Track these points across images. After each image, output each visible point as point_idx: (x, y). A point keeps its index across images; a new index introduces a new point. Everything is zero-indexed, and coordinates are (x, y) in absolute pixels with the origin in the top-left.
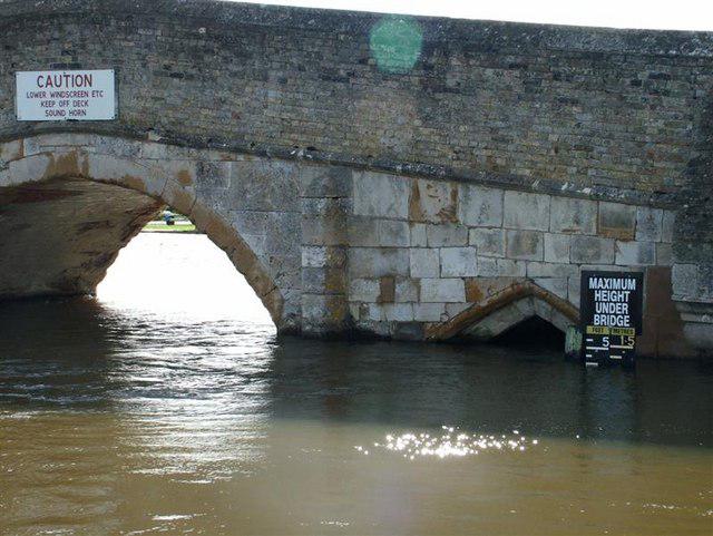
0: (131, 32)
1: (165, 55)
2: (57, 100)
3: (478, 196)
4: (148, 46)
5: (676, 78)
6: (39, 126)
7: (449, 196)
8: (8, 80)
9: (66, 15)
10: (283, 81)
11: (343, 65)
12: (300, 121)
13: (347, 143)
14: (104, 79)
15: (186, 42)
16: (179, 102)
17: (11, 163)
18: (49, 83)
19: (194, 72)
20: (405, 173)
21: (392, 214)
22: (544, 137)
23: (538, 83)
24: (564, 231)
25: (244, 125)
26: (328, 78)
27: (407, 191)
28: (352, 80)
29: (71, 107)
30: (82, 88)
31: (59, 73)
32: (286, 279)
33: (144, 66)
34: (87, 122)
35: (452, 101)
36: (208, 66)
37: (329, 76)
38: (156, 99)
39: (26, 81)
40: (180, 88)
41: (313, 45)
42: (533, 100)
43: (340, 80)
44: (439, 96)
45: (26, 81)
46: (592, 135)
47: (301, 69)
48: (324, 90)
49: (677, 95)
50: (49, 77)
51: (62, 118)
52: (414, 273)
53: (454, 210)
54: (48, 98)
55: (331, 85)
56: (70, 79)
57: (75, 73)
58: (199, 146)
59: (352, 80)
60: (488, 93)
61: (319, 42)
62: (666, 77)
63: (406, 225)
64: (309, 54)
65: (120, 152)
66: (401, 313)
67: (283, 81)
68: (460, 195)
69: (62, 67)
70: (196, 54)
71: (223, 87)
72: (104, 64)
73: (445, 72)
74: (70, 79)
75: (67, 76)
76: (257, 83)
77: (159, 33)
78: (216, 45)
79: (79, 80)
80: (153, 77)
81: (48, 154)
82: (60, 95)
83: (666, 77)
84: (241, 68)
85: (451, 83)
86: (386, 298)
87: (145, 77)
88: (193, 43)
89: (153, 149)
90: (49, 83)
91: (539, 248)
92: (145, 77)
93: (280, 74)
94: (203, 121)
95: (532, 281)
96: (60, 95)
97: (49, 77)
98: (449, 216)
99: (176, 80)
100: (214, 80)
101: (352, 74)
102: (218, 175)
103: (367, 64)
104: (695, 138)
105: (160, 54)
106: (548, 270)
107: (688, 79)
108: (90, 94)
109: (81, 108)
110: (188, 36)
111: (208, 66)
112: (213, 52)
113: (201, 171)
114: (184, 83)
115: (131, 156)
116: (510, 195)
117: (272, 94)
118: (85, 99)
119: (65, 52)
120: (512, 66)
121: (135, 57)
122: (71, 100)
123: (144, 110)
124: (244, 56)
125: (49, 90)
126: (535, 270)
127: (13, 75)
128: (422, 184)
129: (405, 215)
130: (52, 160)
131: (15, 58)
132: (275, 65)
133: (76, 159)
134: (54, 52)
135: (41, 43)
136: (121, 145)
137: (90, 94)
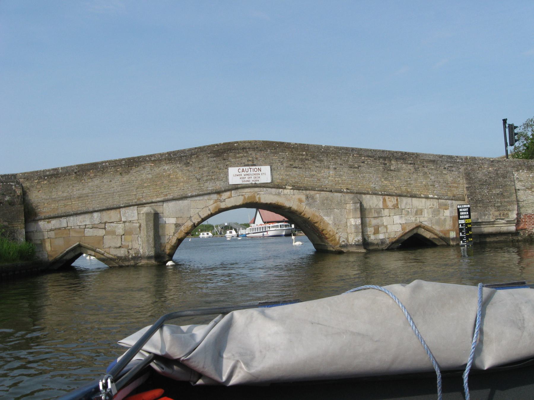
0: (276, 154)
1: (290, 161)
2: (247, 177)
3: (405, 200)
4: (283, 158)
5: (454, 167)
6: (239, 186)
7: (395, 200)
8: (225, 170)
9: (249, 148)
10: (335, 169)
11: (357, 164)
12: (342, 180)
13: (360, 187)
14: (266, 169)
15: (298, 157)
17: (226, 200)
18: (243, 171)
19: (300, 166)
20: (382, 195)
21: (377, 207)
22: (422, 183)
23: (418, 168)
24: (430, 208)
25: (321, 182)
26: (351, 167)
27: (382, 200)
28: (360, 168)
29: (253, 179)
30: (257, 172)
31: (247, 168)
32: (340, 230)
34: (260, 184)
35: (393, 174)
36: (307, 164)
37: (351, 167)
38: (287, 175)
41: (345, 158)
42: (417, 173)
43: (356, 168)
44: (389, 172)
46: (435, 182)
47: (341, 164)
48: (351, 171)
49: (455, 171)
50: (243, 169)
51: (249, 183)
52: (385, 224)
53: (397, 204)
54: (243, 176)
55: (353, 169)
56: (252, 170)
57: (254, 167)
58: (306, 189)
59: (360, 168)
60: (404, 171)
62: (452, 167)
63: (382, 210)
64: (344, 160)
65: (274, 193)
66: (381, 236)
67: (335, 169)
68: (399, 200)
69: (248, 165)
70: (302, 160)
71: (313, 171)
72: (265, 164)
73: (390, 165)
74: (252, 170)
75: (251, 169)
76: (325, 169)
77: (287, 154)
78: (310, 158)
79: (256, 170)
80: (285, 168)
81: (242, 195)
82: (247, 175)
83: (452, 167)
84: (319, 165)
85: (392, 168)
87: (282, 168)
88: (301, 157)
89: (288, 191)
90: (243, 171)
91: (423, 213)
92: (282, 168)
93: (334, 166)
94: (307, 181)
95: (421, 223)
96: (247, 175)
97: (243, 169)
98: (396, 206)
99: (295, 169)
100: (310, 168)
101: (360, 166)
102: (313, 198)
103: (364, 163)
104: (465, 182)
106: (426, 219)
107: (457, 167)
108: (261, 174)
109: (257, 179)
110: (299, 155)
111: (307, 164)
113: (307, 197)
114: (297, 170)
115: (279, 194)
116: (414, 199)
117: (331, 172)
118: (259, 176)
120: (411, 164)
121: (278, 162)
122: (253, 177)
123: (282, 179)
124: (321, 161)
125: (243, 173)
126: (422, 219)
127: (227, 168)
128: (387, 197)
129: (382, 207)
130: (245, 198)
131: (228, 163)
132: (332, 164)
133: (255, 197)
134: (244, 160)
135: (239, 158)
136: (274, 190)
137: (261, 174)
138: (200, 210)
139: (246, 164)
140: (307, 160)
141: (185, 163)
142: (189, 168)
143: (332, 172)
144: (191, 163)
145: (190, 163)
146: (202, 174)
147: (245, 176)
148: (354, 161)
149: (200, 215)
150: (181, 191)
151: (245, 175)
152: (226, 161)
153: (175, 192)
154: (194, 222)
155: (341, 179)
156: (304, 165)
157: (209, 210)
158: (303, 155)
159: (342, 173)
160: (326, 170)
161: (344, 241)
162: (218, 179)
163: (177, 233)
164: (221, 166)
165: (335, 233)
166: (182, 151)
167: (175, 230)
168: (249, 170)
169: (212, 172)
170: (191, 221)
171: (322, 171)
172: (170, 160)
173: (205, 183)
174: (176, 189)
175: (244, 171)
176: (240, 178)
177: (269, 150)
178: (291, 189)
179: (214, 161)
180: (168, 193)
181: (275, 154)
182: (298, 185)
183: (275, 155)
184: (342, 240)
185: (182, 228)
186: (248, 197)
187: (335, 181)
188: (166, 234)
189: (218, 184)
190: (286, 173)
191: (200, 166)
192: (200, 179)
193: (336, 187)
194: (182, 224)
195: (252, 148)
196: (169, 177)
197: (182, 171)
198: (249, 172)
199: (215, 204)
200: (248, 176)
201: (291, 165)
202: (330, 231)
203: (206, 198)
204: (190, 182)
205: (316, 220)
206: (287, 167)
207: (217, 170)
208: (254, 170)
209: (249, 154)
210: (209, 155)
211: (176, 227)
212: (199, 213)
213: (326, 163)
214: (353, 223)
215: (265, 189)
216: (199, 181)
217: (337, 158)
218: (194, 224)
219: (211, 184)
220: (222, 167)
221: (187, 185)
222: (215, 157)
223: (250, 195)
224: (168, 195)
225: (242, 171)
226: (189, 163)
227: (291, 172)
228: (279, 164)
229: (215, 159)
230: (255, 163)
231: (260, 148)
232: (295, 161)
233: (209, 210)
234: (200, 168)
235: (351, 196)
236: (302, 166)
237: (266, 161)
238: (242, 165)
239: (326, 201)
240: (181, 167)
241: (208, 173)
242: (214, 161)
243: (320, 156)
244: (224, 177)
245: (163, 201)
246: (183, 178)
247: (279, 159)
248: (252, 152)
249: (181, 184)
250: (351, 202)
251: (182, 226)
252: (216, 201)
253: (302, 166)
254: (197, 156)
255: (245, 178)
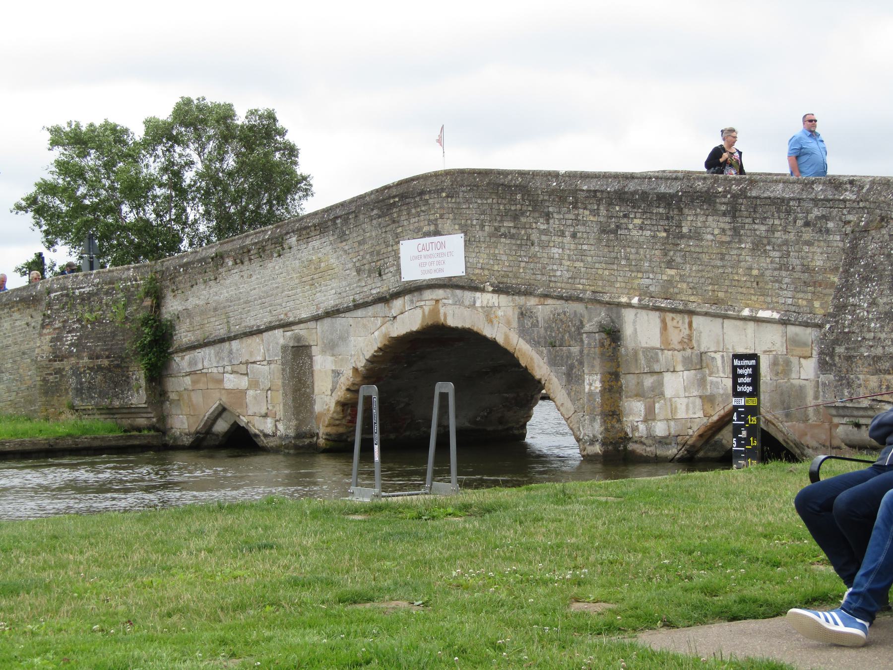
7: (687, 326)
14: (455, 242)
30: (441, 251)
39: (408, 249)
45: (408, 249)
53: (690, 338)
58: (519, 293)
63: (660, 352)
66: (660, 429)
70: (515, 217)
86: (650, 416)
109: (441, 267)
124: (548, 216)
128: (669, 316)
129: (658, 346)
202: (562, 404)
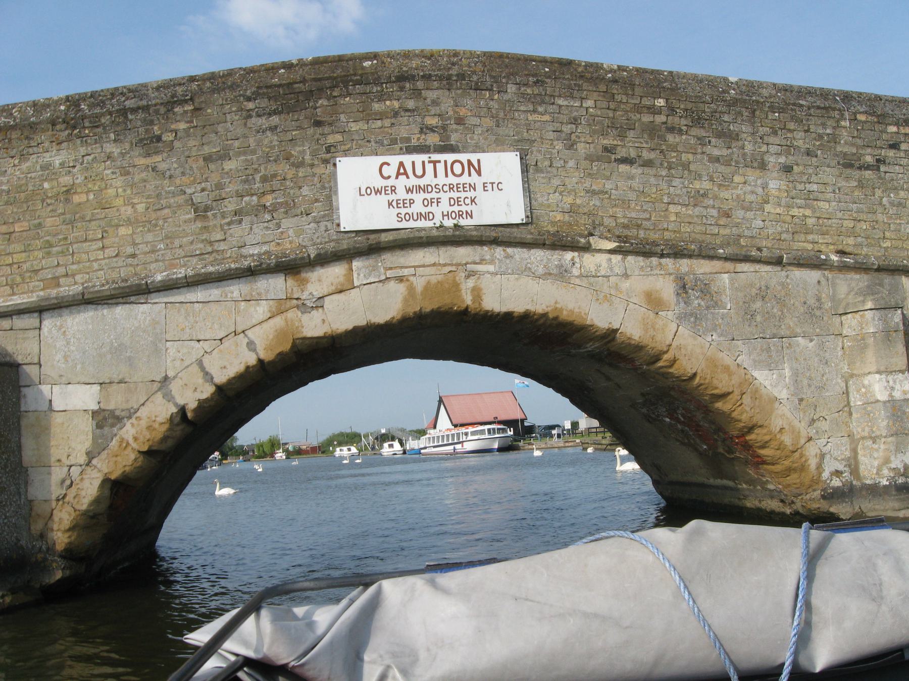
0: (543, 102)
1: (604, 134)
2: (419, 197)
4: (575, 121)
6: (384, 238)
8: (320, 170)
9: (427, 77)
10: (788, 169)
11: (869, 150)
13: (887, 244)
15: (635, 117)
16: (632, 196)
17: (326, 299)
18: (401, 171)
19: (646, 155)
25: (737, 225)
26: (849, 166)
28: (883, 168)
29: (445, 207)
30: (465, 179)
31: (418, 158)
32: (823, 425)
33: (571, 146)
36: (674, 148)
37: (849, 163)
38: (594, 193)
40: (631, 178)
41: (824, 125)
43: (868, 167)
47: (808, 153)
48: (847, 178)
51: (429, 224)
54: (401, 194)
55: (856, 174)
56: (440, 167)
57: (450, 157)
58: (678, 254)
59: (883, 168)
61: (830, 123)
64: (820, 137)
65: (541, 270)
67: (788, 169)
70: (652, 131)
71: (700, 176)
72: (499, 145)
74: (440, 167)
75: (435, 163)
77: (589, 103)
78: (684, 122)
79: (458, 168)
80: (584, 164)
81: (400, 279)
84: (725, 152)
87: (571, 163)
88: (646, 118)
90: (401, 171)
92: (571, 163)
93: (782, 160)
99: (623, 168)
100: (686, 166)
102: (705, 290)
103: (899, 149)
105: (595, 132)
108: (479, 187)
109: (464, 208)
110: (638, 109)
111: (674, 148)
112: (680, 130)
113: (683, 287)
114: (636, 171)
115: (562, 275)
117: (773, 185)
118: (472, 194)
119: (425, 129)
121: (551, 135)
122: (445, 197)
123: (573, 210)
124: (730, 137)
130: (411, 289)
131: (331, 139)
132: (773, 149)
133: (456, 286)
134: (407, 129)
135: (381, 116)
137: (479, 187)
138: (207, 346)
139: (414, 142)
140: (671, 130)
141: (141, 140)
142: (158, 158)
143: (775, 184)
144: (168, 137)
145: (164, 138)
146: (219, 186)
147: (410, 196)
148: (859, 142)
149: (208, 368)
150: (120, 262)
151: (409, 190)
152: (327, 129)
153: (96, 265)
154: (181, 402)
155: (814, 212)
156: (662, 152)
157: (251, 345)
158: (657, 111)
159: (814, 187)
160: (752, 175)
161: (838, 473)
162: (289, 208)
163: (104, 455)
164: (303, 150)
165: (802, 441)
166: (130, 90)
167: (94, 439)
168: (429, 168)
169: (264, 179)
170: (169, 397)
171: (737, 179)
172: (74, 127)
173: (229, 224)
174: (100, 255)
175: (405, 173)
176: (390, 204)
177: (511, 88)
178: (612, 252)
179: (273, 129)
180: (61, 271)
181: (540, 104)
182: (642, 234)
183: (540, 109)
184: (833, 469)
185: (129, 431)
186: (427, 287)
187: (788, 219)
188: (53, 459)
189: (291, 232)
190: (587, 185)
191: (207, 150)
192: (207, 209)
193: (796, 246)
194: (123, 414)
195: (440, 78)
196: (67, 200)
197: (128, 173)
198: (429, 179)
199: (278, 321)
200: (423, 195)
201: (606, 149)
202: (782, 429)
203: (236, 294)
204: (165, 220)
205: (722, 384)
206: (590, 158)
207: (283, 168)
208: (449, 169)
209: (429, 101)
210: (251, 105)
211: (99, 426)
212: (206, 362)
213: (749, 147)
214: (882, 396)
215: (499, 251)
216: (205, 217)
217: (791, 125)
218: (183, 410)
219: (259, 232)
220: (308, 157)
221: (150, 237)
222: (275, 112)
223: (434, 280)
224: (62, 281)
225: (398, 174)
226: (159, 139)
227: (608, 179)
228: (559, 146)
229: (275, 120)
230: (454, 139)
231: (475, 78)
232: (622, 136)
233: (251, 345)
234: (208, 159)
235: (860, 280)
236: (652, 155)
237: (501, 131)
238: (397, 147)
239: (758, 305)
240: (122, 155)
241: (246, 181)
242: (273, 129)
243: (726, 118)
244: (317, 201)
245: (41, 310)
246: (133, 205)
247: (557, 125)
248: (440, 92)
249: (123, 231)
250: (869, 305)
251: (128, 426)
252: (280, 308)
253: (652, 155)
254: (196, 109)
255: (412, 202)
